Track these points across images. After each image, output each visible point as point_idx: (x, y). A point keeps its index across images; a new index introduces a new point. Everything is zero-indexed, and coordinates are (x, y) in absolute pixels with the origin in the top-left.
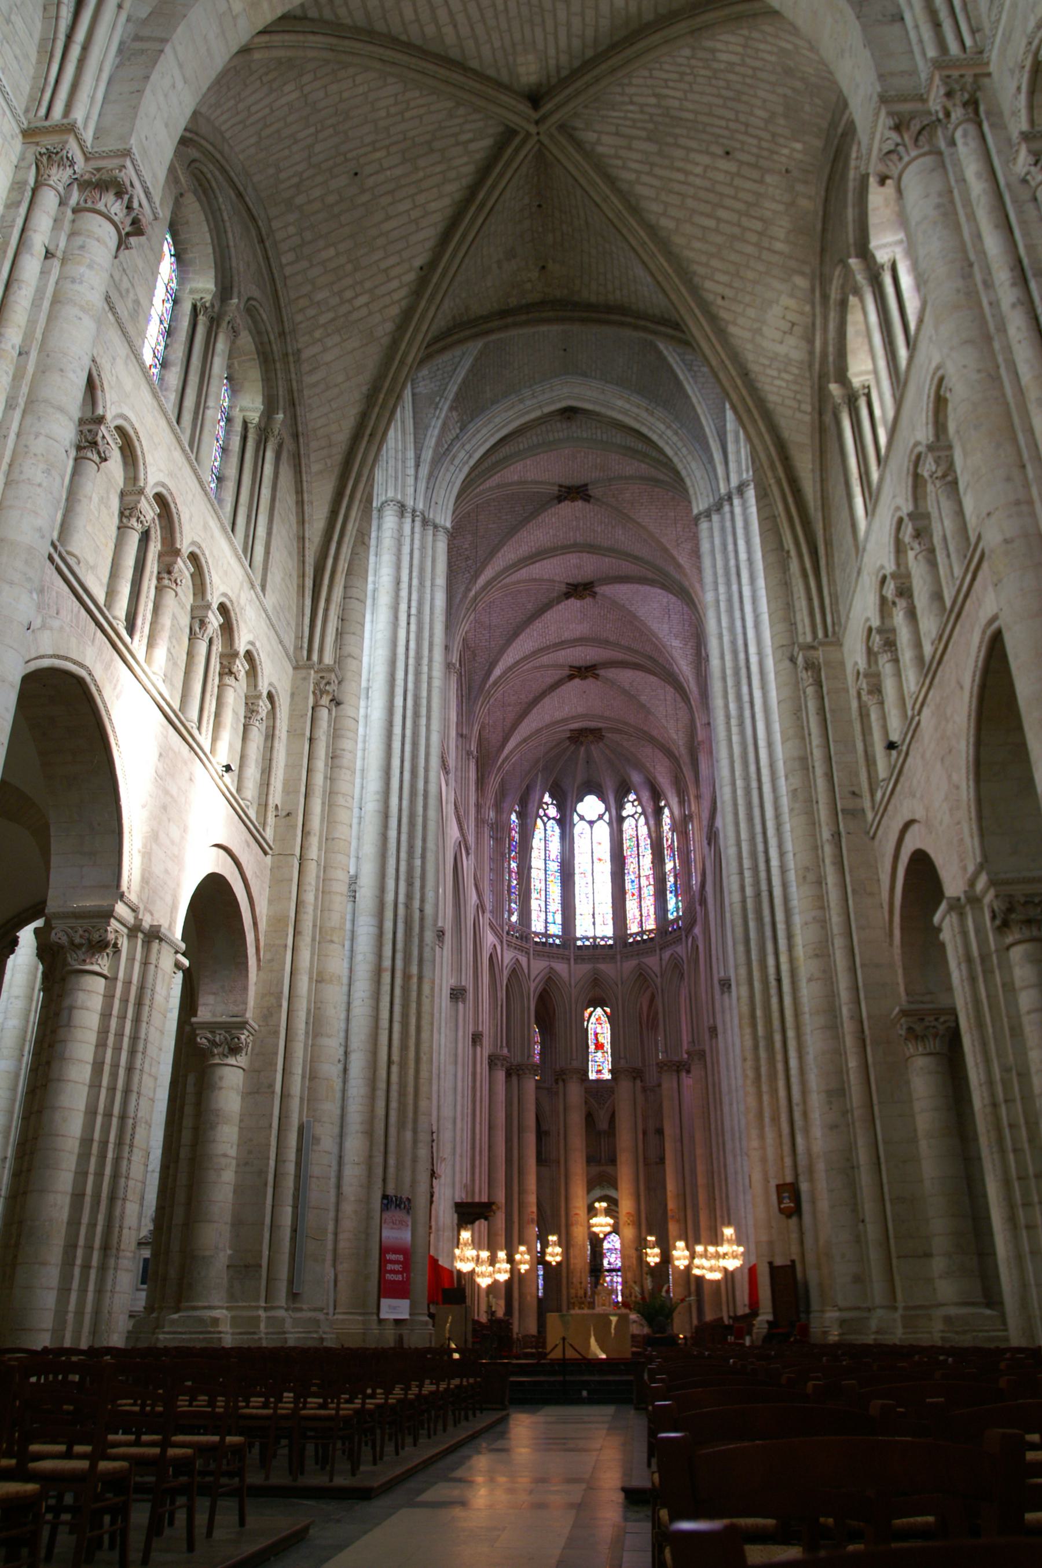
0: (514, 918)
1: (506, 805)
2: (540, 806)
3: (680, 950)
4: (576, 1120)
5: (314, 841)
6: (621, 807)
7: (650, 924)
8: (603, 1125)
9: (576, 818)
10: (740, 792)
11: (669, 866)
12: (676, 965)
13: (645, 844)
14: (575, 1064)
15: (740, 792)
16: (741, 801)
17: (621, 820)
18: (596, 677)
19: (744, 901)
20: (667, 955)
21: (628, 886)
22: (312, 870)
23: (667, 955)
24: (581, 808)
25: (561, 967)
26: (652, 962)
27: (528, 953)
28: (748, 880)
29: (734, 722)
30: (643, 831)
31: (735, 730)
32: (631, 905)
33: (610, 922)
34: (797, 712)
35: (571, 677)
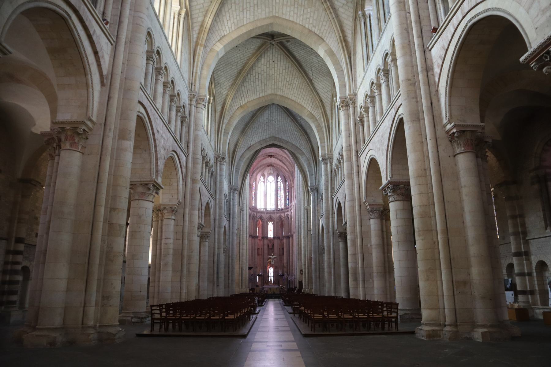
0: (254, 205)
1: (252, 180)
2: (260, 179)
3: (289, 213)
4: (266, 247)
5: (241, 232)
6: (277, 179)
7: (283, 207)
8: (270, 247)
9: (267, 181)
10: (299, 207)
11: (287, 194)
12: (287, 217)
13: (282, 188)
14: (266, 236)
15: (299, 207)
16: (299, 208)
17: (277, 182)
18: (274, 157)
19: (298, 225)
20: (286, 214)
21: (278, 197)
22: (241, 235)
23: (286, 214)
24: (268, 179)
25: (263, 215)
26: (283, 215)
27: (256, 212)
28: (299, 222)
29: (299, 194)
30: (282, 185)
31: (299, 196)
32: (279, 202)
33: (274, 205)
34: (304, 215)
35: (268, 157)
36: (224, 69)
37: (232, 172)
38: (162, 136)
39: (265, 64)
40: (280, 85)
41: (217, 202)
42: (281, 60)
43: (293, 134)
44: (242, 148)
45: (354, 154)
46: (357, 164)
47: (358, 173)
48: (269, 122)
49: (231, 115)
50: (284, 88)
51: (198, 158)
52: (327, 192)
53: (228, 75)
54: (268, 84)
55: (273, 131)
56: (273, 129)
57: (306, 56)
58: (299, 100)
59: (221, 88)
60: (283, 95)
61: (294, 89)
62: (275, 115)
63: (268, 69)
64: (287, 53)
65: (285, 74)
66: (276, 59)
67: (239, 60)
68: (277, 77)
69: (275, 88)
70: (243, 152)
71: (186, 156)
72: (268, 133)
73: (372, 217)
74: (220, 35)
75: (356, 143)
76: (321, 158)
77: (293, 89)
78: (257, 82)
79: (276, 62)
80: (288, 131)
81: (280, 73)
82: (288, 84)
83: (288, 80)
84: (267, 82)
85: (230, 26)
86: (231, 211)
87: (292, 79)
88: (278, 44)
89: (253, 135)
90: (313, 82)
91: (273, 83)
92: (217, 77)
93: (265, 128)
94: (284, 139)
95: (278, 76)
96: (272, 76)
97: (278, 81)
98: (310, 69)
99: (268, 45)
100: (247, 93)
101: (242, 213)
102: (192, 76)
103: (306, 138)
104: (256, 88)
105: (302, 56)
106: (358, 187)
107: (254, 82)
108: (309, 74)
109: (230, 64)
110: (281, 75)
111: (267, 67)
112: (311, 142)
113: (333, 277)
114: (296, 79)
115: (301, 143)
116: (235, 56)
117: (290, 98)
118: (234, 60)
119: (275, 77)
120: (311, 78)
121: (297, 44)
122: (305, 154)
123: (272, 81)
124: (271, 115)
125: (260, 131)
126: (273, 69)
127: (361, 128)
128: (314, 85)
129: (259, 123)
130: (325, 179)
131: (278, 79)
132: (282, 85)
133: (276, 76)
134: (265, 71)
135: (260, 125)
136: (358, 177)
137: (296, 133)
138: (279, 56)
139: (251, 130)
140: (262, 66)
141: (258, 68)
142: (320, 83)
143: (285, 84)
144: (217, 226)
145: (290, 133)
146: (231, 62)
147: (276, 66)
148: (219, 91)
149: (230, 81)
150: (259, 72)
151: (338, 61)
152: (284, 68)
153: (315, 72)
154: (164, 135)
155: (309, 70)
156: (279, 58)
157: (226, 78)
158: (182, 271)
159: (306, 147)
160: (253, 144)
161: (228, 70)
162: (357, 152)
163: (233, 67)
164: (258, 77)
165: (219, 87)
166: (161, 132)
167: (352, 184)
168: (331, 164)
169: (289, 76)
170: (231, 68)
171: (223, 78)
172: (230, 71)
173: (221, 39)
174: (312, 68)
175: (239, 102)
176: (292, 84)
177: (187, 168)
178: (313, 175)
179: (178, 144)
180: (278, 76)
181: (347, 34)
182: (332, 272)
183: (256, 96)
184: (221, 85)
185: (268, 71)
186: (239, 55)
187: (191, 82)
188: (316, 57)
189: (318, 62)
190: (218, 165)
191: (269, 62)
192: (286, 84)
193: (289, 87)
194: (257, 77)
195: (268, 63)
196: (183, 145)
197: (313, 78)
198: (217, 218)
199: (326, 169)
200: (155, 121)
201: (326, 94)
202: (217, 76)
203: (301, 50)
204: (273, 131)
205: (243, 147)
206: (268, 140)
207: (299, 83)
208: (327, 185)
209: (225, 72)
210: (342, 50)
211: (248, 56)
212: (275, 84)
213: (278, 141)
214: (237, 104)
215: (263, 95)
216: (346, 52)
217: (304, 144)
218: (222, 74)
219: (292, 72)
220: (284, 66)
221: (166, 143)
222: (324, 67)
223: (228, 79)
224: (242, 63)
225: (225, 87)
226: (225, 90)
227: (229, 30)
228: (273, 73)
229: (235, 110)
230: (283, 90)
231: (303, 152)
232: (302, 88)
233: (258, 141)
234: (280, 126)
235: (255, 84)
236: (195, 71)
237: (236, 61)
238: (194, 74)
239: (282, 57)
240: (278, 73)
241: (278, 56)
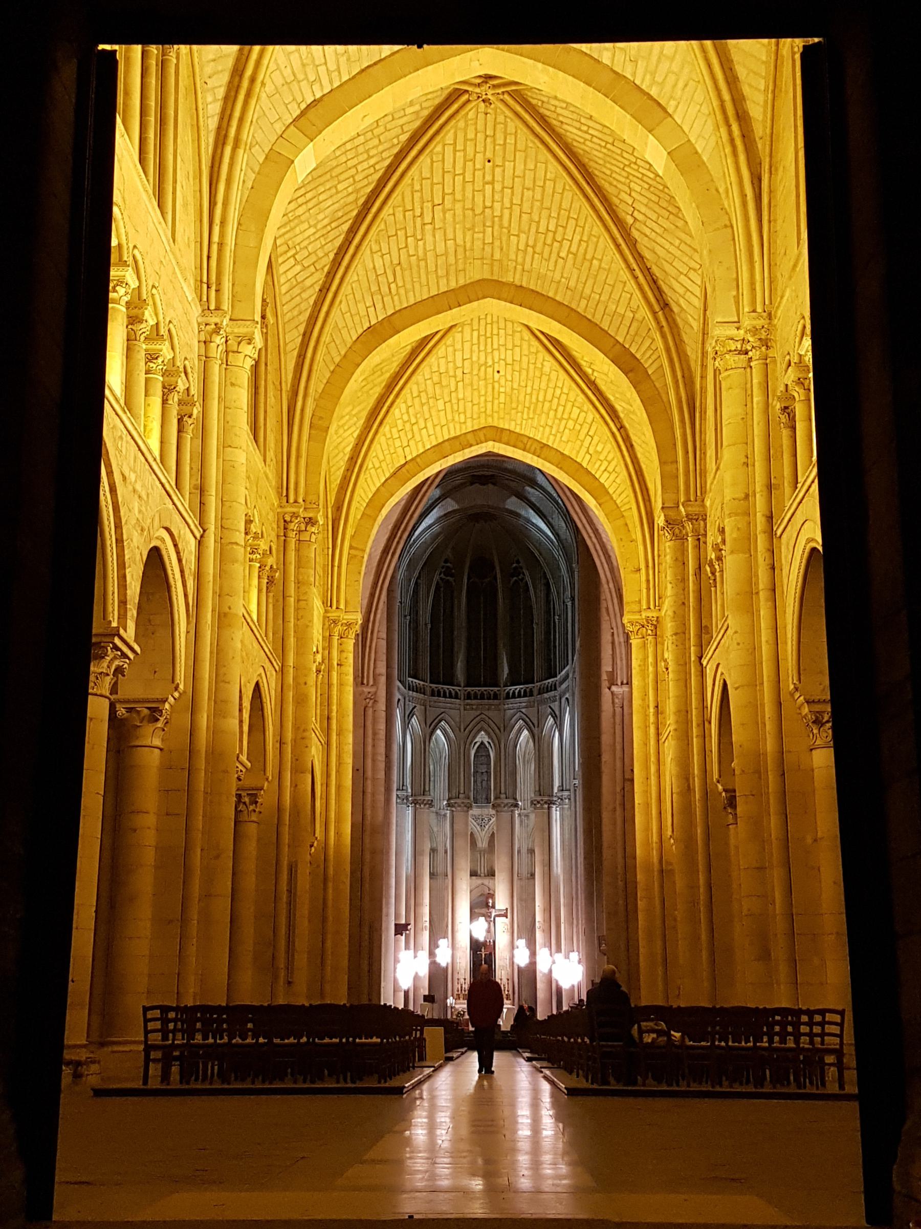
5: (369, 782)
18: (494, 484)
35: (472, 484)
36: (309, 196)
37: (336, 564)
38: (134, 491)
40: (513, 248)
41: (290, 679)
43: (566, 416)
44: (373, 471)
45: (759, 528)
46: (768, 561)
47: (774, 590)
48: (475, 372)
49: (337, 360)
50: (528, 259)
51: (236, 544)
52: (683, 644)
53: (321, 216)
54: (468, 245)
55: (489, 405)
56: (490, 399)
58: (584, 303)
59: (297, 262)
60: (524, 284)
62: (495, 346)
63: (469, 187)
64: (538, 129)
65: (532, 208)
67: (361, 158)
68: (501, 217)
69: (497, 256)
70: (378, 485)
71: (195, 537)
72: (469, 415)
73: (818, 742)
74: (299, 99)
75: (770, 487)
76: (662, 518)
77: (561, 261)
78: (429, 238)
79: (499, 161)
80: (547, 405)
81: (512, 203)
82: (545, 244)
84: (464, 238)
85: (332, 66)
86: (334, 708)
87: (557, 226)
88: (506, 97)
89: (413, 421)
90: (635, 234)
91: (489, 240)
93: (461, 396)
94: (531, 436)
95: (507, 212)
96: (483, 212)
97: (505, 231)
98: (627, 189)
99: (468, 101)
100: (391, 279)
101: (370, 712)
102: (209, 257)
103: (613, 434)
104: (425, 260)
105: (595, 140)
106: (772, 641)
108: (622, 206)
109: (328, 176)
110: (516, 209)
111: (464, 182)
112: (630, 447)
113: (705, 954)
114: (572, 223)
115: (596, 452)
117: (551, 294)
120: (630, 220)
122: (611, 491)
123: (484, 232)
124: (482, 348)
125: (440, 405)
126: (488, 188)
127: (786, 433)
128: (638, 246)
129: (436, 378)
130: (676, 595)
131: (506, 224)
132: (522, 247)
133: (497, 213)
134: (458, 196)
135: (440, 383)
136: (770, 604)
137: (576, 411)
138: (511, 140)
139: (405, 402)
140: (448, 178)
142: (659, 240)
143: (531, 243)
144: (288, 765)
145: (552, 413)
146: (333, 168)
147: (498, 177)
148: (290, 275)
149: (330, 238)
151: (714, 192)
152: (529, 183)
154: (138, 487)
156: (510, 148)
157: (315, 226)
158: (184, 920)
159: (614, 463)
160: (414, 455)
161: (321, 198)
162: (770, 518)
164: (433, 218)
165: (292, 261)
166: (132, 477)
167: (753, 630)
168: (700, 539)
169: (545, 213)
170: (334, 191)
171: (306, 225)
172: (330, 202)
173: (303, 113)
175: (363, 312)
176: (556, 244)
177: (199, 576)
178: (639, 570)
179: (174, 504)
180: (507, 212)
181: (746, 90)
182: (704, 937)
183: (425, 289)
184: (297, 253)
185: (469, 194)
187: (205, 279)
190: (292, 545)
191: (473, 160)
193: (546, 255)
194: (428, 219)
195: (470, 164)
196: (183, 503)
197: (635, 219)
198: (289, 735)
199: (680, 559)
200: (117, 448)
201: (682, 278)
204: (489, 405)
205: (377, 465)
206: (469, 437)
207: (585, 238)
208: (684, 617)
209: (310, 205)
210: (728, 150)
211: (395, 141)
212: (497, 243)
213: (507, 444)
214: (356, 318)
215: (453, 285)
216: (742, 158)
217: (605, 453)
218: (300, 211)
219: (557, 197)
220: (529, 175)
221: (143, 509)
223: (325, 231)
224: (372, 170)
225: (313, 258)
226: (312, 269)
227: (331, 82)
228: (488, 204)
229: (349, 343)
231: (603, 485)
233: (434, 443)
234: (515, 386)
236: (216, 238)
237: (350, 164)
238: (215, 247)
240: (507, 204)
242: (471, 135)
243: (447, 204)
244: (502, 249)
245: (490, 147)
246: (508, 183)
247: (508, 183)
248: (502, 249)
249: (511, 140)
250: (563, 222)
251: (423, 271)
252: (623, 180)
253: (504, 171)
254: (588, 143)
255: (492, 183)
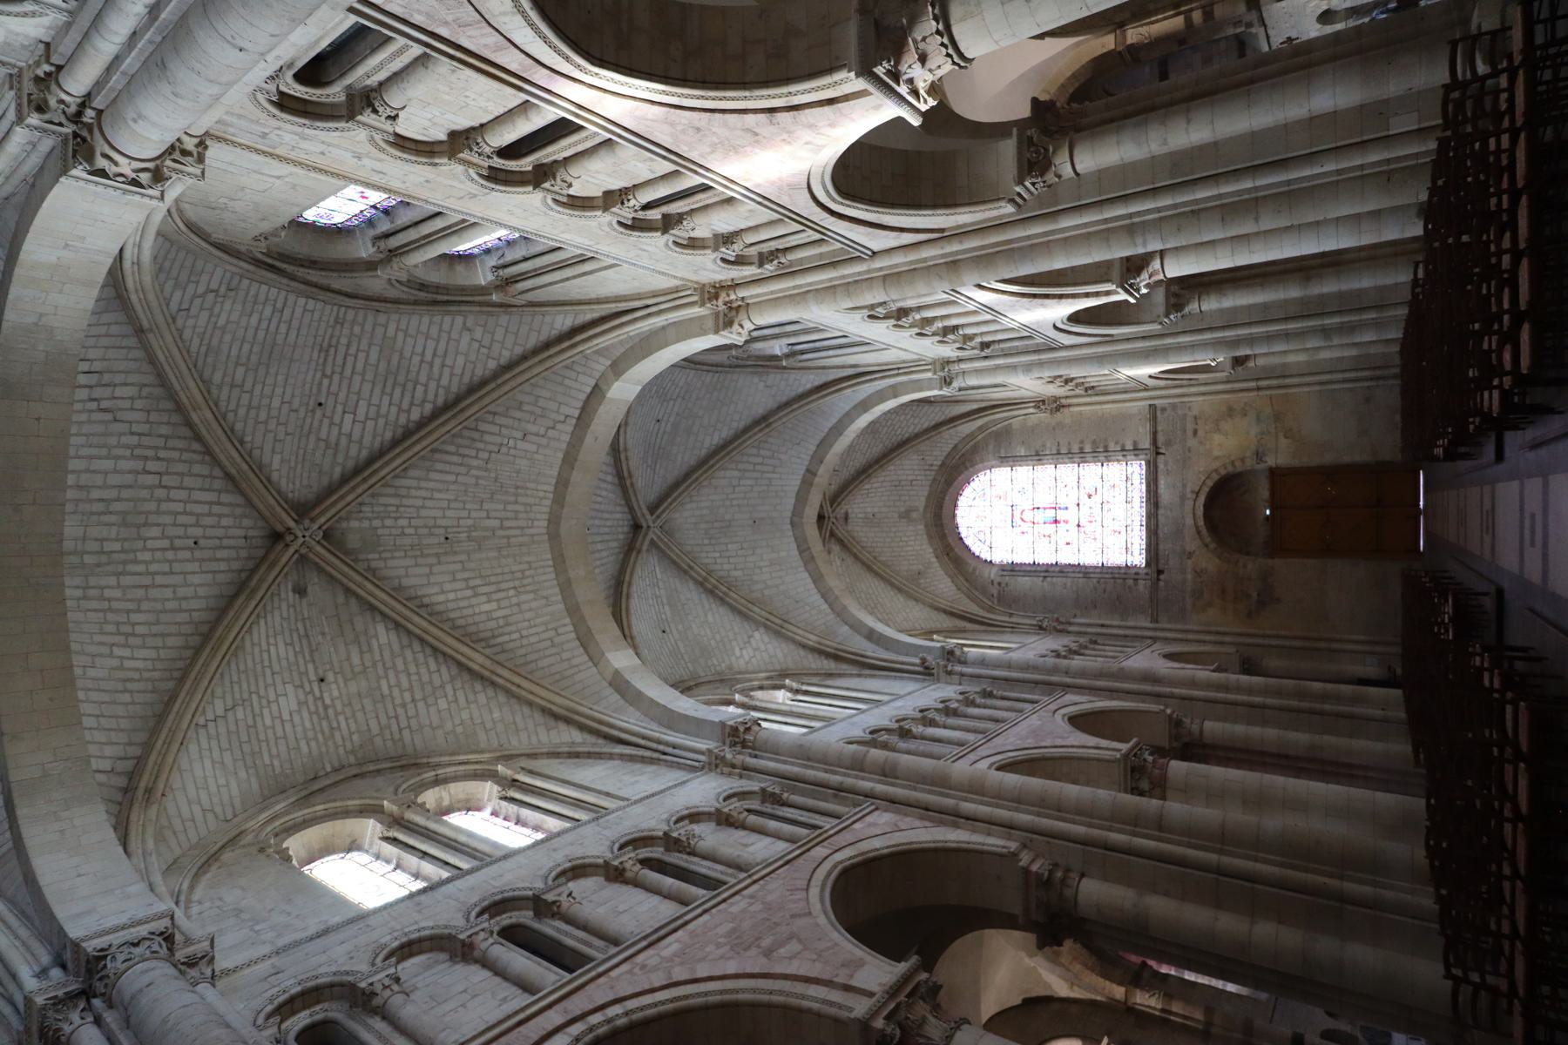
36: (261, 334)
39: (189, 507)
40: (103, 581)
42: (209, 576)
50: (94, 605)
53: (227, 338)
57: (276, 668)
61: (111, 655)
66: (207, 554)
68: (135, 562)
69: (88, 559)
79: (198, 554)
83: (135, 617)
91: (108, 546)
92: (257, 295)
95: (141, 568)
97: (120, 568)
98: (230, 703)
107: (137, 452)
110: (146, 581)
114: (152, 654)
116: (279, 391)
118: (270, 381)
119: (135, 551)
121: (300, 626)
126: (165, 543)
132: (107, 593)
133: (141, 556)
138: (223, 566)
141: (182, 474)
142: (208, 763)
143: (115, 605)
150: (166, 480)
152: (182, 592)
153: (233, 728)
155: (224, 698)
156: (214, 566)
157: (224, 330)
161: (246, 347)
163: (240, 371)
169: (151, 617)
174: (240, 714)
184: (217, 296)
186: (276, 403)
188: (299, 703)
189: (286, 716)
191: (197, 525)
192: (117, 611)
202: (262, 297)
203: (286, 644)
207: (146, 675)
212: (104, 559)
218: (254, 320)
219: (174, 629)
220: (189, 591)
222: (283, 748)
228: (150, 544)
230: (85, 598)
232: (131, 692)
235: (128, 453)
239: (221, 578)
240: (154, 567)
241: (223, 560)
242: (225, 522)
243: (160, 493)
244: (98, 565)
245: (211, 543)
246: (177, 567)
247: (177, 567)
248: (98, 565)
249: (223, 566)
250: (150, 642)
251: (94, 451)
252: (237, 696)
253: (188, 561)
254: (257, 650)
255: (173, 548)
